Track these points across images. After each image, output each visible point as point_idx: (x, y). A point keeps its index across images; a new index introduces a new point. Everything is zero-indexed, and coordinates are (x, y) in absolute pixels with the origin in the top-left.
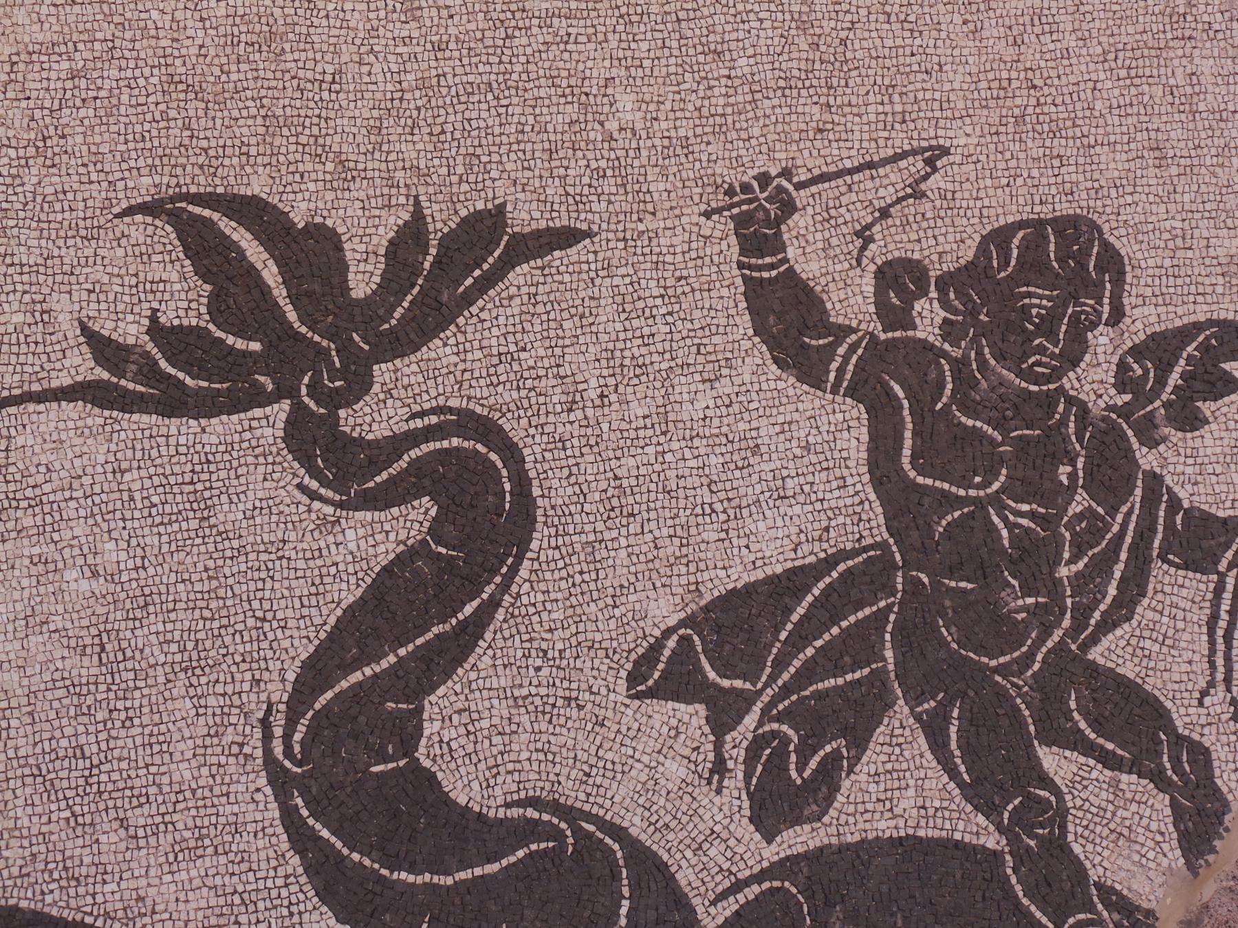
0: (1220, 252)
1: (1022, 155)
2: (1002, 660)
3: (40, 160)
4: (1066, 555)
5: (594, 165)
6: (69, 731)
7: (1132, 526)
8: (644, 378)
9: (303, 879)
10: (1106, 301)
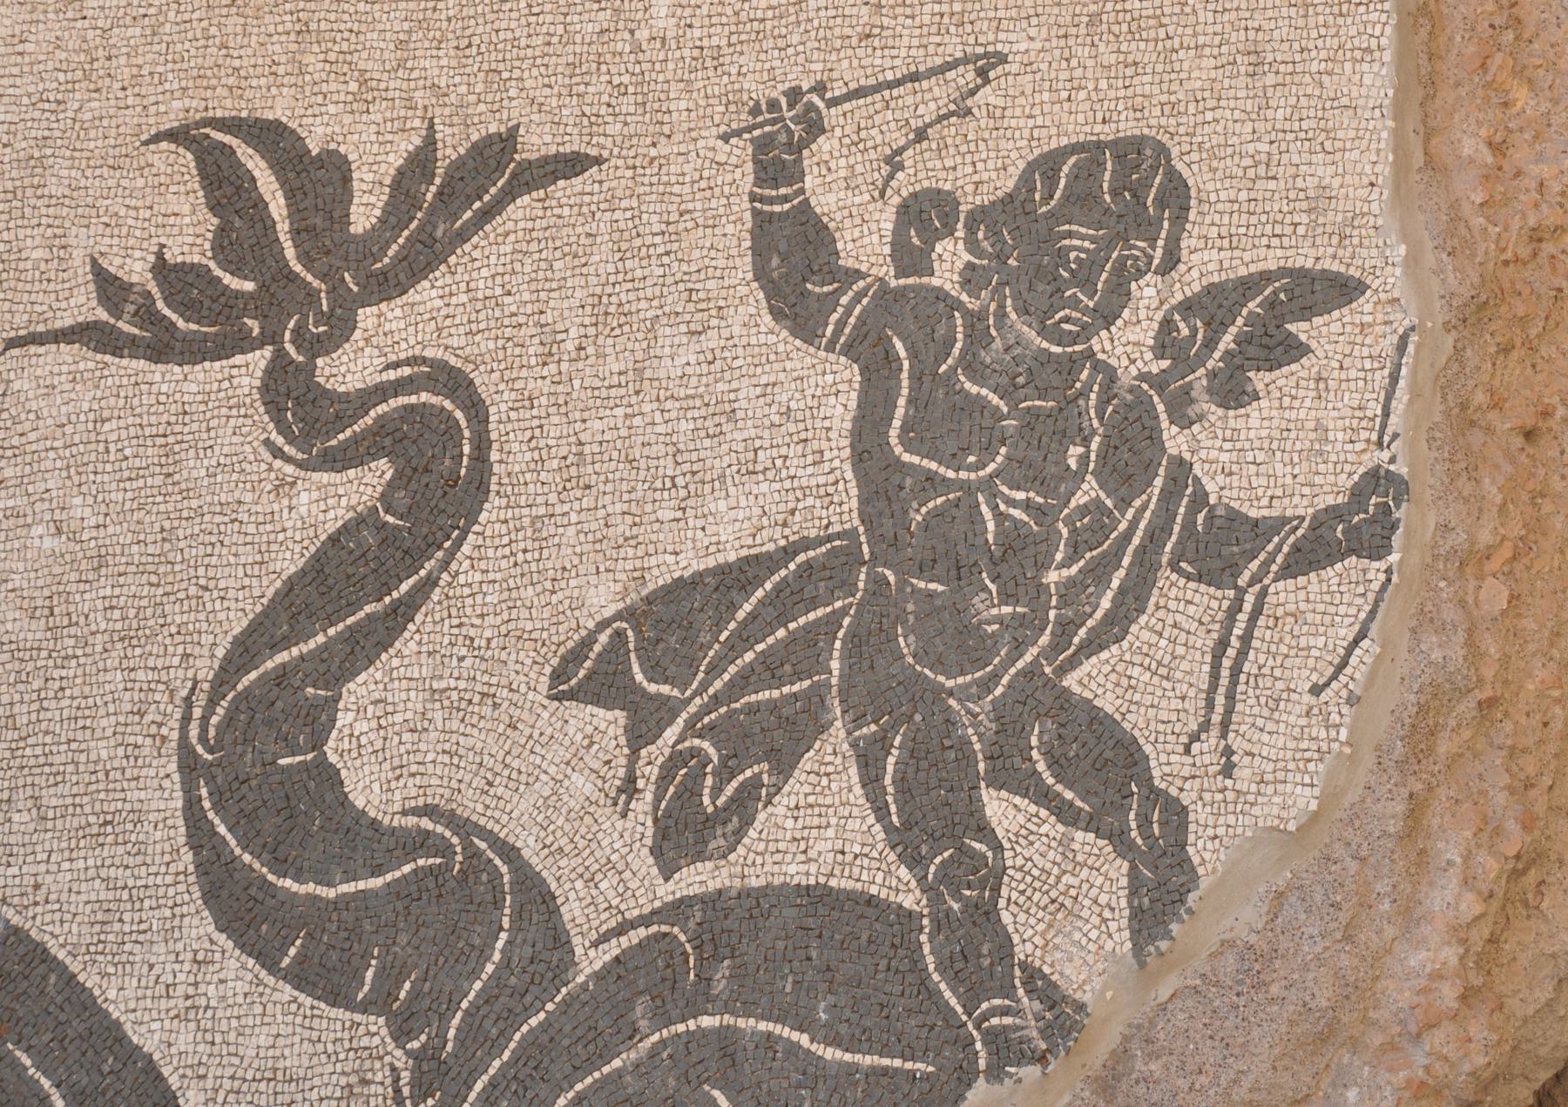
1: (1090, 63)
4: (1059, 557)
9: (192, 879)
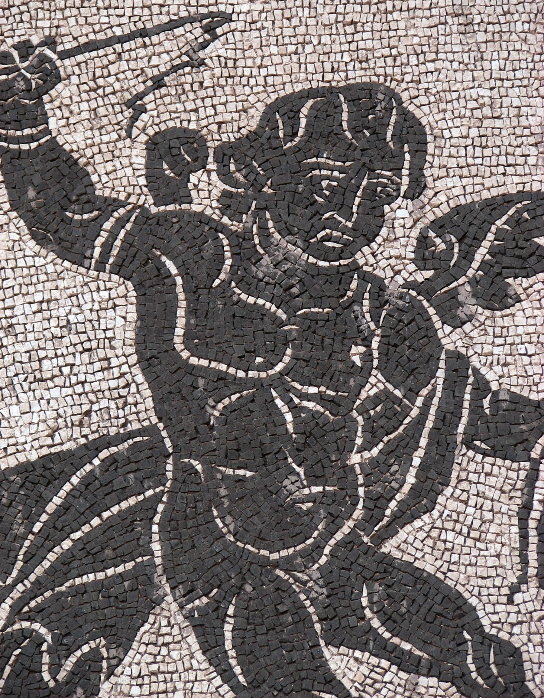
0: (532, 121)
2: (284, 553)
4: (359, 441)
7: (433, 410)
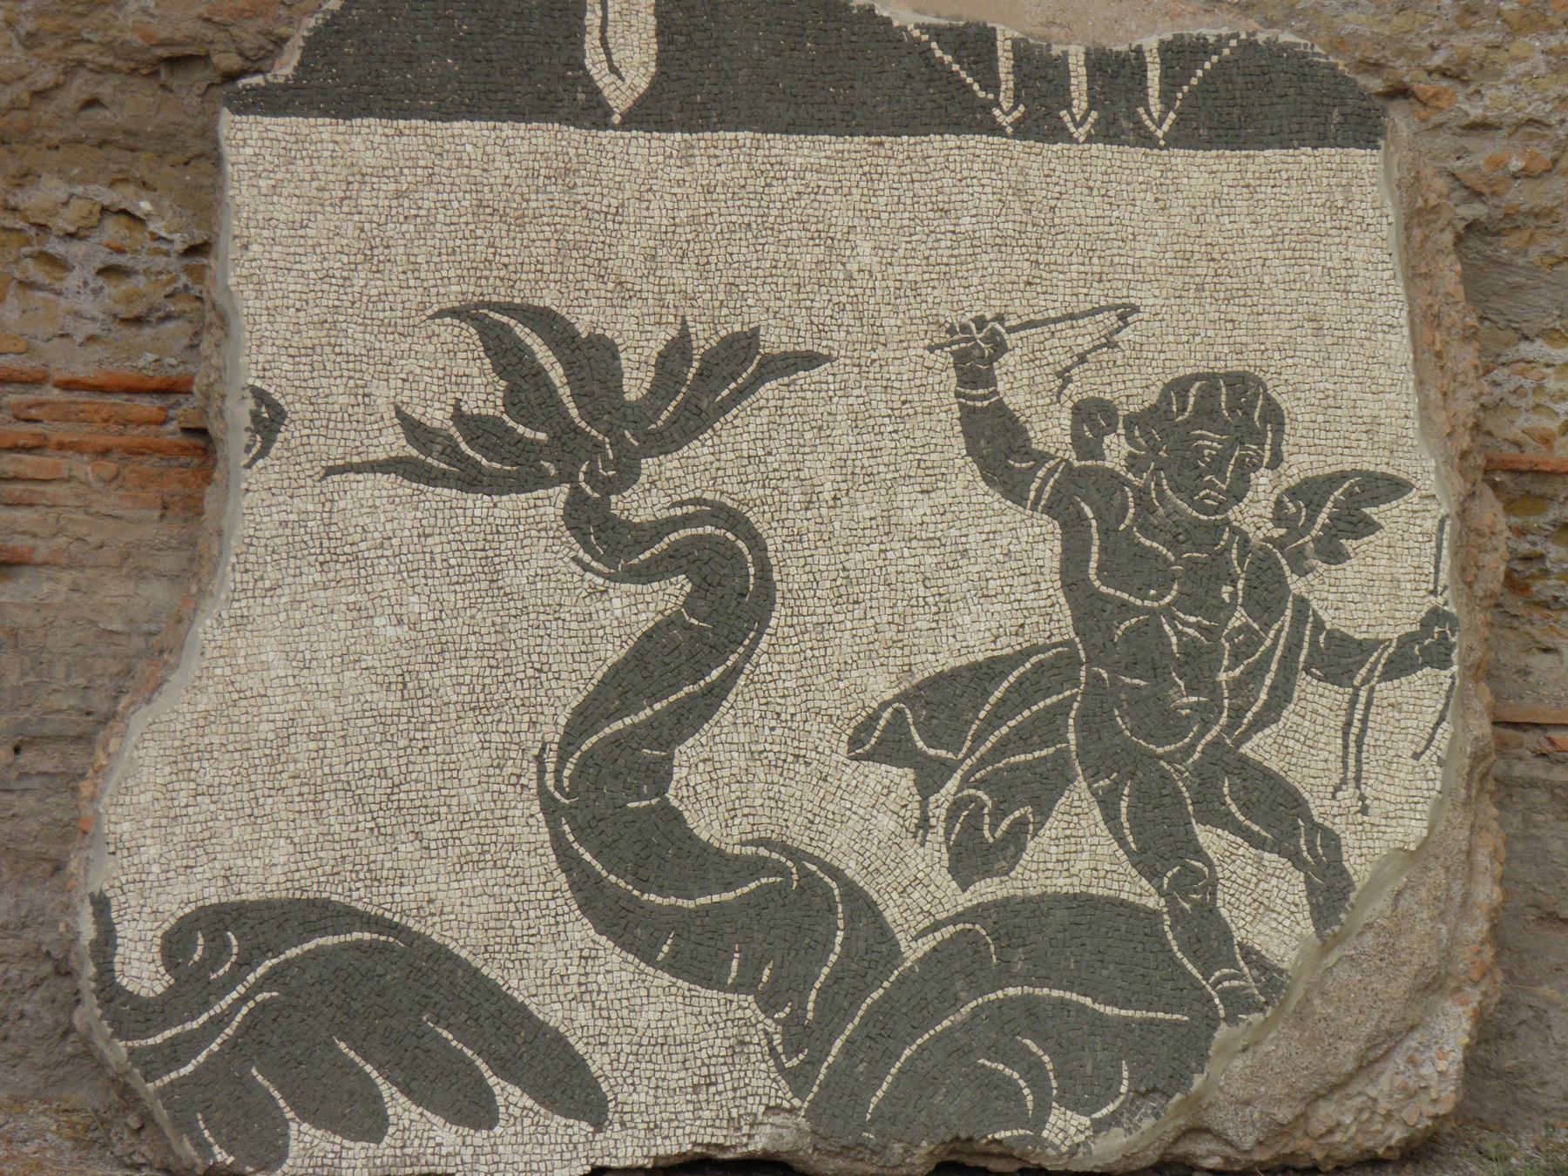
1: (1200, 317)
2: (1167, 748)
3: (367, 266)
4: (1226, 663)
5: (835, 300)
6: (375, 754)
7: (1282, 641)
8: (871, 486)
9: (568, 894)
10: (1267, 447)
